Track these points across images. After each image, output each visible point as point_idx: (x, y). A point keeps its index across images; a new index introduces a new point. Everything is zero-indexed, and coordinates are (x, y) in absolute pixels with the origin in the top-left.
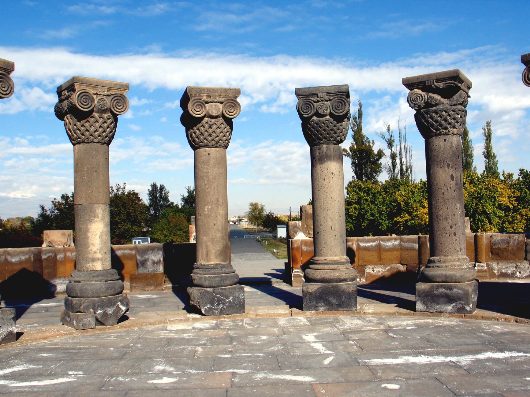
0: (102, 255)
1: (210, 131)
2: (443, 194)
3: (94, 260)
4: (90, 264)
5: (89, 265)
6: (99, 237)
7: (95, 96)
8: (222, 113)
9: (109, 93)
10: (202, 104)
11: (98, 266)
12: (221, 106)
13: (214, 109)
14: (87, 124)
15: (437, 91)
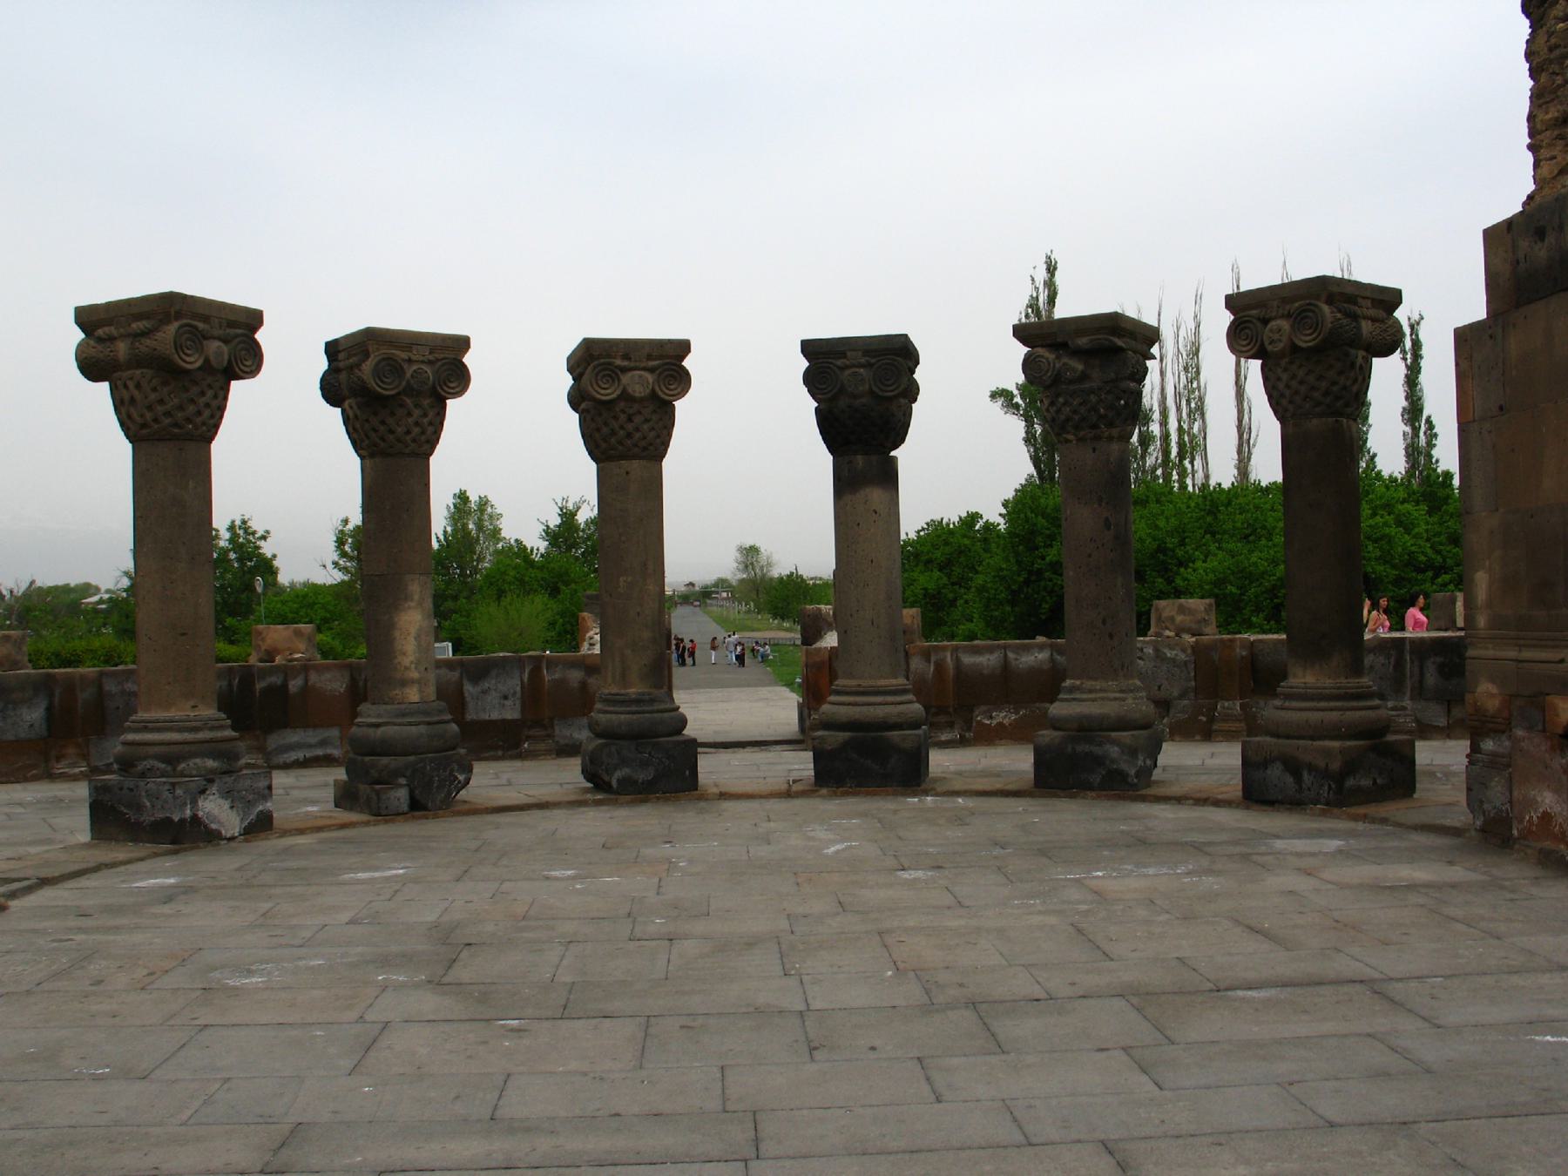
0: (419, 672)
1: (630, 427)
2: (1090, 556)
3: (404, 683)
4: (397, 692)
5: (395, 692)
6: (413, 639)
7: (405, 366)
8: (653, 390)
9: (431, 357)
10: (613, 374)
11: (413, 695)
12: (650, 378)
13: (638, 383)
14: (390, 421)
15: (1078, 353)
